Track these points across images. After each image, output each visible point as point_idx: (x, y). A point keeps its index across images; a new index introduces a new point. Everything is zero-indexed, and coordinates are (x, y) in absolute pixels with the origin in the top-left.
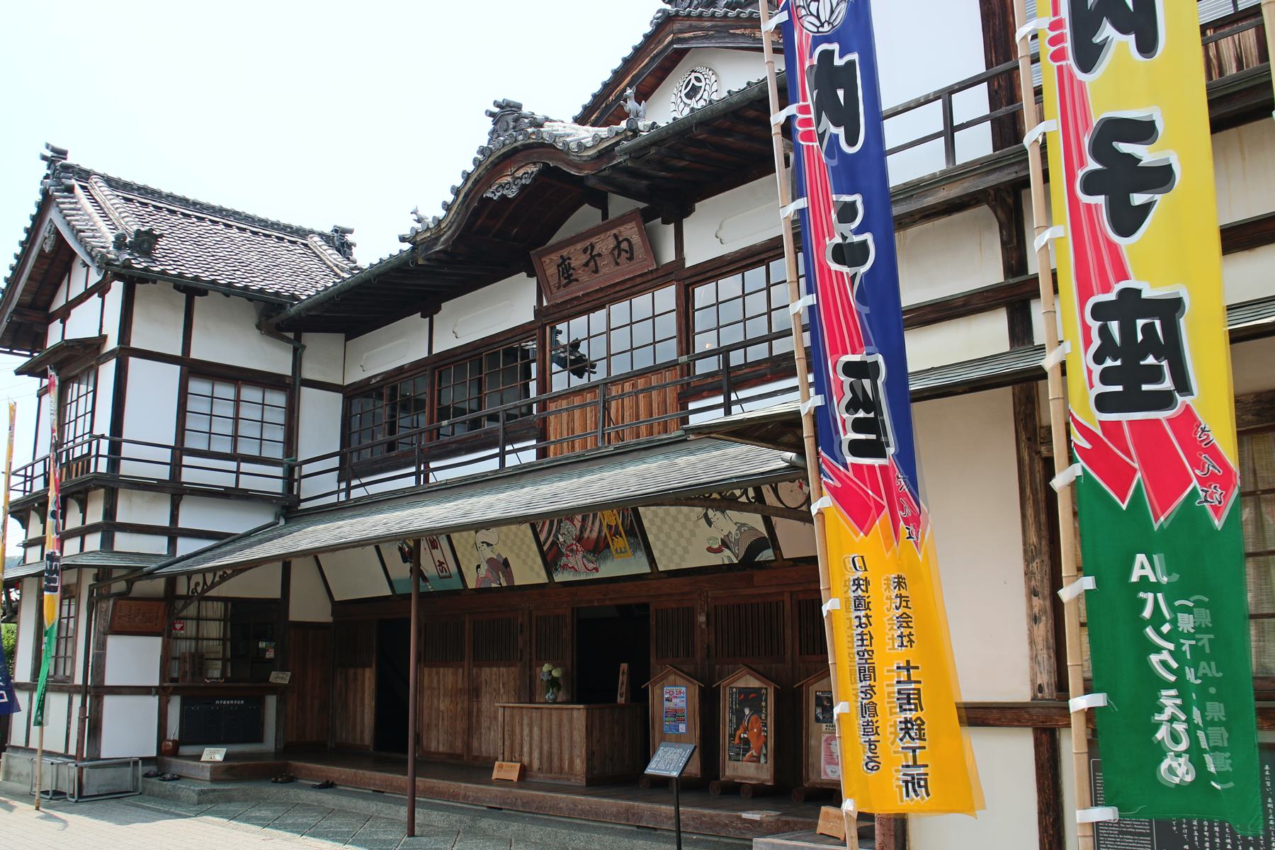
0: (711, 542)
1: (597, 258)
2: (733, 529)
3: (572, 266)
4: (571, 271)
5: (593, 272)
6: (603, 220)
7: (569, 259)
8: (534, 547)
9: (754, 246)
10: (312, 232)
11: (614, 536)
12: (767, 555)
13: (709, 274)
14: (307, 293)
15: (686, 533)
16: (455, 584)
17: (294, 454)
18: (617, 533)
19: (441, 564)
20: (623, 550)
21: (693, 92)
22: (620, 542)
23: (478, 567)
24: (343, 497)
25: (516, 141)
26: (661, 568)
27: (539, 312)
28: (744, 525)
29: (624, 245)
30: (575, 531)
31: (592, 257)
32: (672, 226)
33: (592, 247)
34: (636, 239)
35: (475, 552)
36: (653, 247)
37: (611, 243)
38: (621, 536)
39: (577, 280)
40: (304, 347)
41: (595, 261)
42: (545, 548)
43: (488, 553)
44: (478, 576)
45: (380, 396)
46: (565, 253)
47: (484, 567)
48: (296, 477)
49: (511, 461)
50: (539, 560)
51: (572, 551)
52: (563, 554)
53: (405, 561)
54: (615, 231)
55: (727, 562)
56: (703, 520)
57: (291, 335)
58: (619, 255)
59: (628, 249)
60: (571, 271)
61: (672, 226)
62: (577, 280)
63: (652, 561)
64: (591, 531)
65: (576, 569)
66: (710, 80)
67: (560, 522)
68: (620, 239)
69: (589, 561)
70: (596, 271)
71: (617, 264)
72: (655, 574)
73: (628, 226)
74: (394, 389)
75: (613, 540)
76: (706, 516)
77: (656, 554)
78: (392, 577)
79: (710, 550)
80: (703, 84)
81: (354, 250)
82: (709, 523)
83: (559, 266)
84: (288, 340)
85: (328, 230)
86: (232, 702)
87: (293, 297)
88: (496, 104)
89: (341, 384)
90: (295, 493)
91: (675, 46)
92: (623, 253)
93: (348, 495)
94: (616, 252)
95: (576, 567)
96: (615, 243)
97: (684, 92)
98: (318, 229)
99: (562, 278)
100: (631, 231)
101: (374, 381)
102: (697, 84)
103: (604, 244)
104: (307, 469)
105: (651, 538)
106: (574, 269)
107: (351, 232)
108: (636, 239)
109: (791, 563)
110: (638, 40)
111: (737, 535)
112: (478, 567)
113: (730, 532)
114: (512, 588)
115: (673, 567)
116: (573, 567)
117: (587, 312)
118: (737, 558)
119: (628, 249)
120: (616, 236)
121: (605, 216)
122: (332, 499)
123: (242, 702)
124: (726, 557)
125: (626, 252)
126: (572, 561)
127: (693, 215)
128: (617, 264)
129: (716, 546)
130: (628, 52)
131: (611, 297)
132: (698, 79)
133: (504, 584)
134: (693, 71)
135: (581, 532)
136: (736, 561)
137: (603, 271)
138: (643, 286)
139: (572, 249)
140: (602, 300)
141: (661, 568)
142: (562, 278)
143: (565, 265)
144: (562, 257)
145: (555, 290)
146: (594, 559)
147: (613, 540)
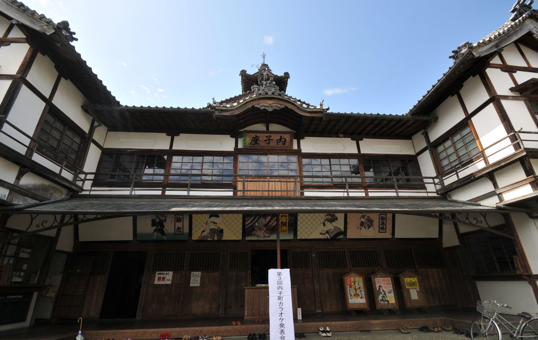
0: (322, 231)
2: (332, 228)
3: (259, 139)
4: (258, 141)
5: (267, 144)
7: (259, 137)
12: (342, 237)
20: (285, 231)
23: (204, 231)
28: (336, 227)
29: (283, 140)
31: (269, 139)
33: (270, 136)
38: (286, 226)
39: (259, 144)
41: (269, 141)
42: (246, 227)
43: (213, 226)
46: (258, 135)
50: (241, 231)
52: (255, 230)
53: (153, 225)
54: (281, 135)
55: (326, 238)
56: (323, 224)
58: (280, 142)
59: (284, 141)
60: (258, 141)
62: (259, 144)
64: (273, 223)
65: (260, 235)
68: (282, 138)
69: (267, 233)
70: (269, 144)
72: (295, 240)
73: (287, 135)
75: (281, 227)
79: (321, 234)
82: (324, 225)
83: (253, 138)
86: (16, 296)
92: (281, 142)
94: (279, 141)
96: (280, 138)
99: (253, 142)
101: (129, 151)
109: (348, 240)
112: (204, 231)
113: (331, 229)
118: (330, 237)
120: (281, 136)
123: (22, 296)
124: (327, 236)
125: (283, 142)
126: (258, 233)
128: (278, 144)
136: (329, 238)
140: (267, 153)
144: (256, 136)
146: (270, 233)
147: (281, 227)
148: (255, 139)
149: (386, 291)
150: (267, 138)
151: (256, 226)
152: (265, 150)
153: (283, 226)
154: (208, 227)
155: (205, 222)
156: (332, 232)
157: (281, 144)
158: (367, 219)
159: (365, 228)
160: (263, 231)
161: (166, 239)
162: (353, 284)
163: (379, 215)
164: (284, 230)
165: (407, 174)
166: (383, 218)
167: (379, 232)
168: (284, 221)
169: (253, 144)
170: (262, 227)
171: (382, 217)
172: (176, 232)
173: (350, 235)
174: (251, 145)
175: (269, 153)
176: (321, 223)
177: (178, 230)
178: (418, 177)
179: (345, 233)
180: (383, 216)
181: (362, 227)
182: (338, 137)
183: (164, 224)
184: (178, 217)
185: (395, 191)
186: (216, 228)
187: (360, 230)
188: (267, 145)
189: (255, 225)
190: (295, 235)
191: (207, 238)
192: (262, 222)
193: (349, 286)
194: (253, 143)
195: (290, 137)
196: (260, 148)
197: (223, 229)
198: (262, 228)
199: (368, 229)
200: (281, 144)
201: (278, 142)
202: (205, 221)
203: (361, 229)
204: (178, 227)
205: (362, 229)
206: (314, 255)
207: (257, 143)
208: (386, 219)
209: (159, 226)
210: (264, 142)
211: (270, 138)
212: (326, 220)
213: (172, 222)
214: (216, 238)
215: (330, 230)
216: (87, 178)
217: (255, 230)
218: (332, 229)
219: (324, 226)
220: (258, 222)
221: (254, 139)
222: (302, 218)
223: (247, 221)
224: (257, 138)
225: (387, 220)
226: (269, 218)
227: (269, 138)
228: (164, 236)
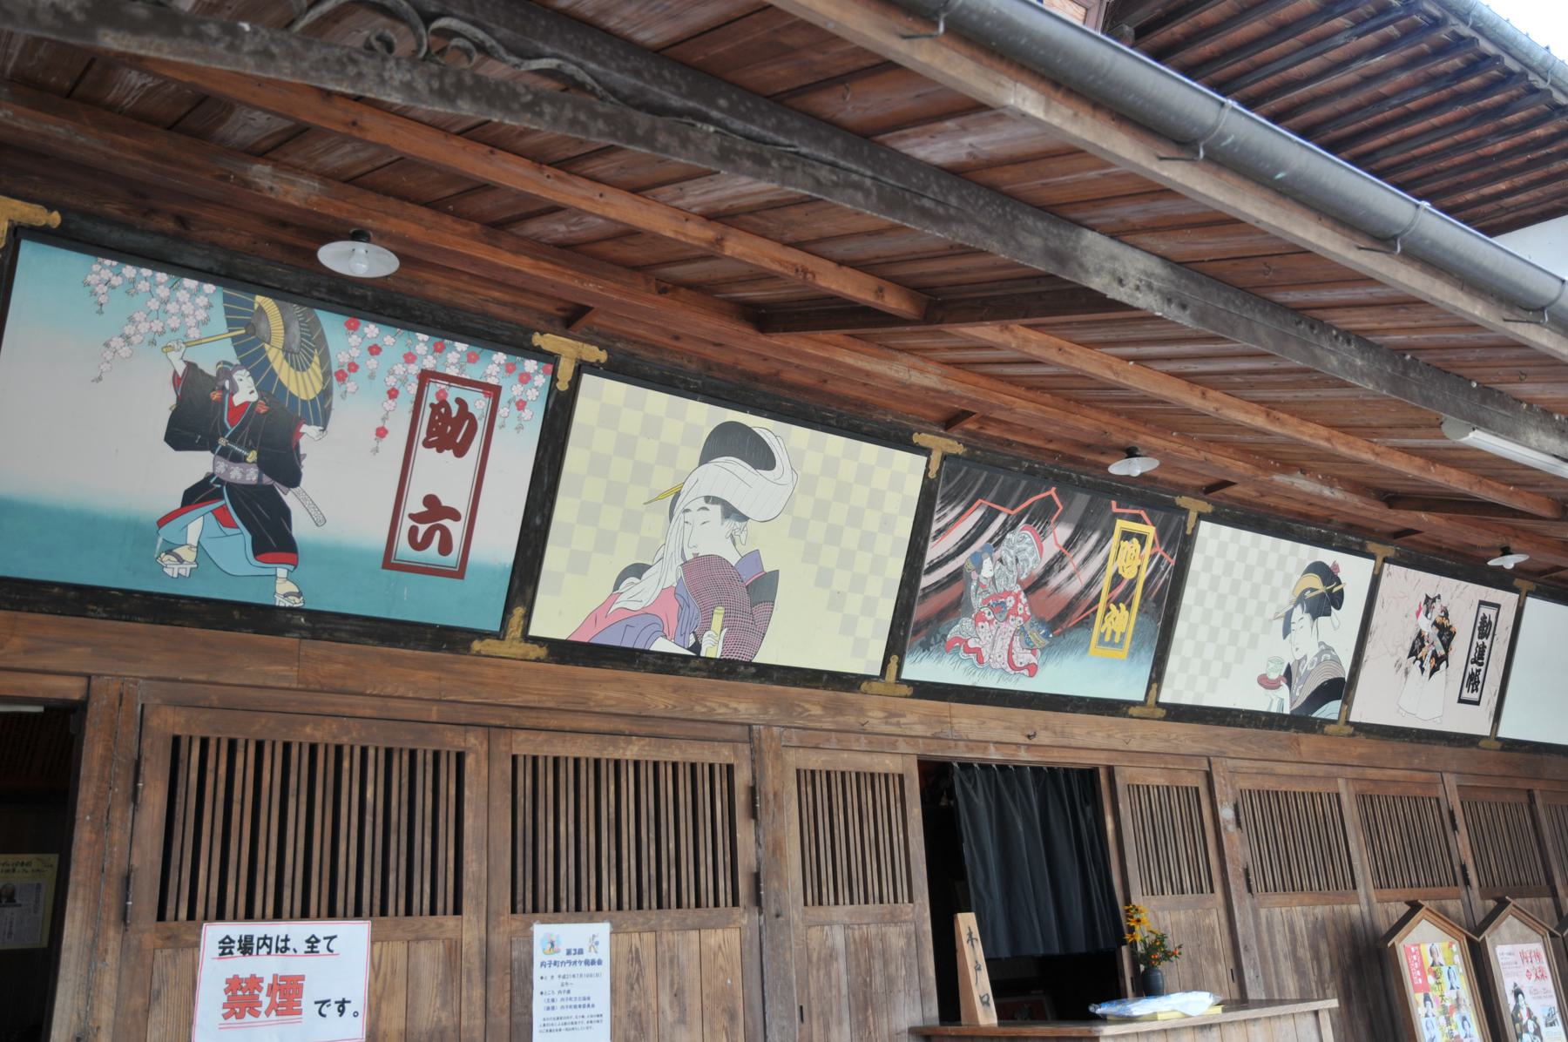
0: (1272, 665)
2: (1312, 651)
11: (1116, 603)
12: (1331, 710)
15: (1244, 638)
18: (1124, 598)
20: (1117, 640)
22: (1121, 621)
23: (638, 570)
28: (1329, 649)
30: (1035, 565)
38: (1129, 607)
42: (926, 581)
47: (664, 576)
64: (1070, 577)
75: (1108, 610)
76: (1288, 617)
82: (1287, 631)
111: (1312, 664)
112: (638, 570)
113: (1305, 657)
116: (977, 651)
124: (1281, 701)
129: (1273, 676)
135: (1049, 570)
147: (1108, 610)
149: (1541, 1014)
151: (979, 584)
153: (1113, 607)
154: (673, 547)
155: (664, 494)
159: (1423, 670)
160: (1015, 623)
161: (296, 602)
162: (1431, 980)
164: (1113, 633)
167: (1461, 701)
168: (1128, 575)
170: (1010, 593)
173: (1368, 707)
177: (423, 528)
184: (443, 403)
186: (733, 559)
189: (974, 575)
190: (1157, 675)
191: (652, 638)
192: (1017, 560)
193: (1419, 997)
197: (775, 574)
202: (663, 481)
204: (431, 501)
206: (1226, 813)
209: (252, 456)
213: (381, 433)
214: (712, 648)
215: (1299, 662)
220: (997, 555)
223: (940, 531)
226: (1063, 532)
228: (282, 572)
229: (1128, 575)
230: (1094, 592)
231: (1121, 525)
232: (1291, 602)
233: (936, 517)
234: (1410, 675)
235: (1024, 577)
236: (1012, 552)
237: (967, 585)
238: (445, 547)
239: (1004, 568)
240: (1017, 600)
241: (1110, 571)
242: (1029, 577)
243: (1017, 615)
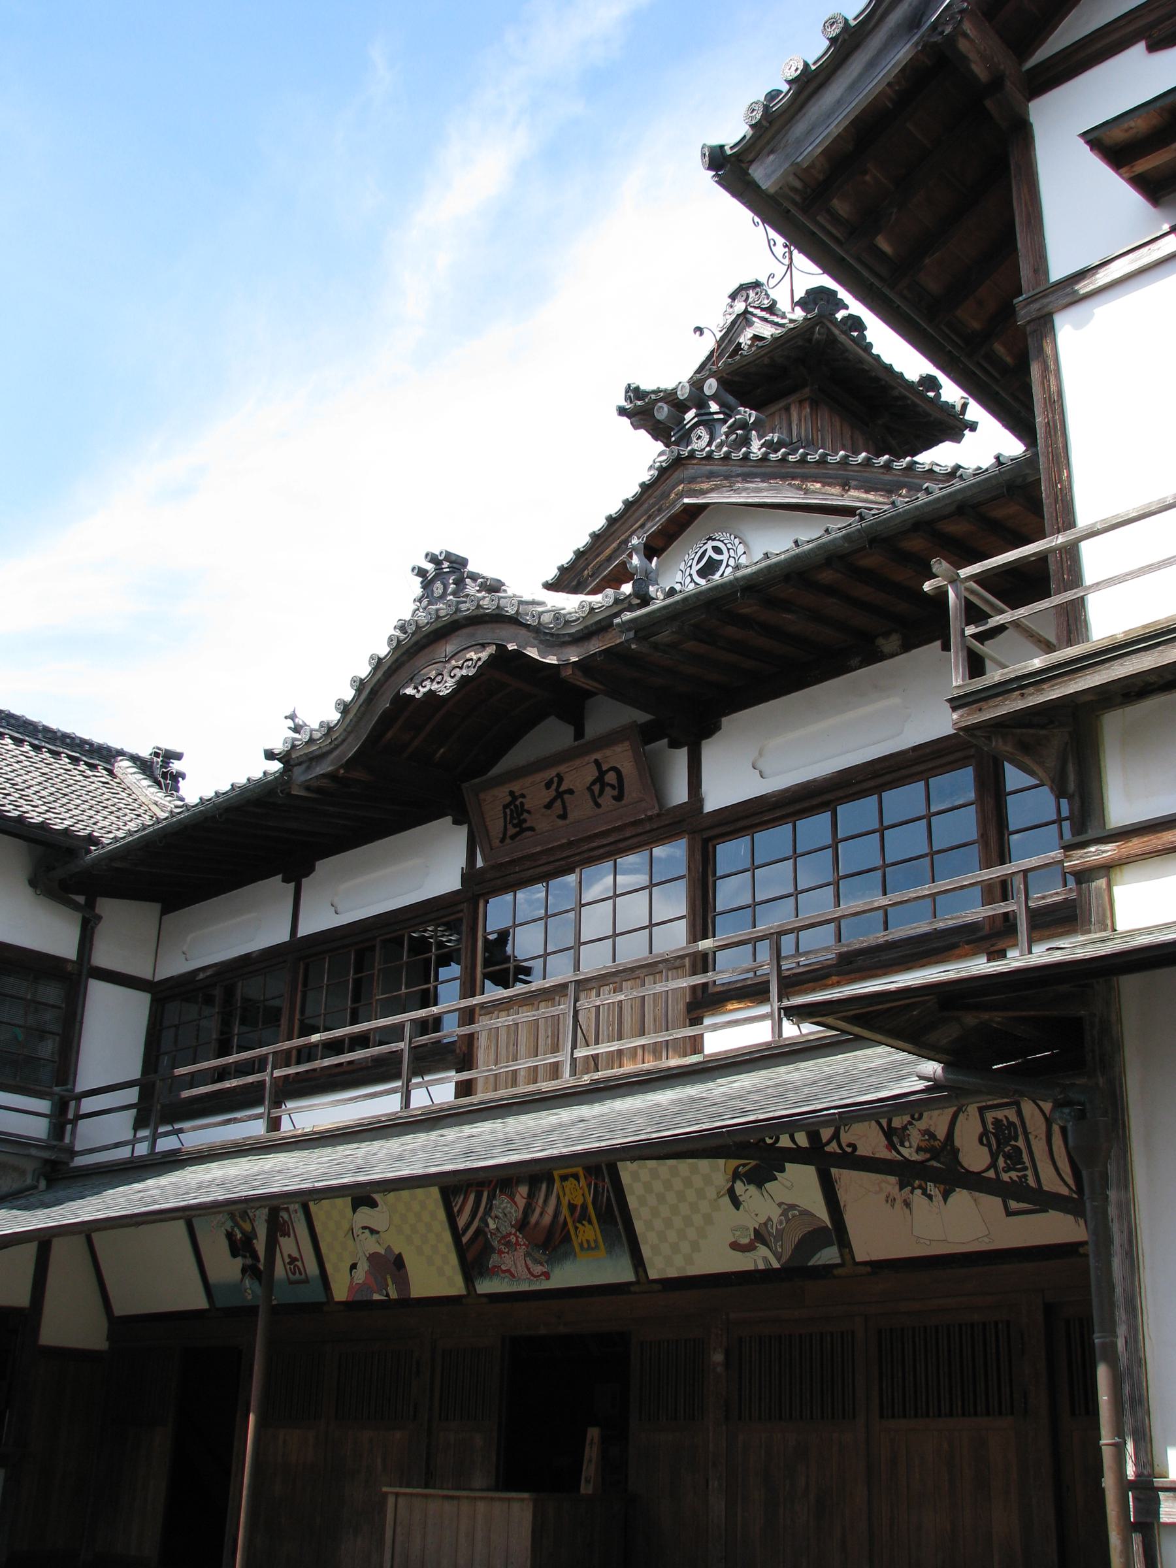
0: (737, 1233)
1: (566, 796)
2: (775, 1213)
4: (525, 815)
5: (559, 817)
6: (576, 739)
7: (523, 796)
8: (447, 1237)
9: (814, 781)
10: (121, 753)
11: (580, 1222)
13: (740, 824)
14: (110, 836)
15: (698, 1219)
16: (313, 1294)
17: (71, 1082)
18: (584, 1217)
19: (293, 1260)
20: (593, 1245)
21: (710, 568)
22: (589, 1232)
23: (354, 1267)
24: (142, 1149)
25: (458, 610)
26: (653, 1274)
27: (469, 875)
28: (792, 1207)
29: (611, 778)
30: (516, 1213)
31: (560, 795)
32: (685, 750)
33: (561, 779)
34: (627, 767)
35: (350, 1242)
36: (654, 780)
37: (591, 774)
38: (590, 1222)
39: (532, 829)
40: (99, 918)
42: (465, 1239)
43: (371, 1245)
44: (352, 1279)
45: (209, 1000)
46: (516, 787)
47: (363, 1267)
48: (70, 1116)
49: (419, 1100)
51: (508, 1244)
52: (493, 1250)
53: (234, 1254)
54: (597, 756)
55: (761, 1266)
56: (727, 1199)
57: (81, 899)
59: (614, 782)
60: (525, 815)
61: (685, 750)
62: (532, 829)
63: (638, 1262)
64: (541, 1214)
66: (736, 552)
67: (491, 1198)
68: (605, 768)
69: (537, 1262)
70: (563, 816)
71: (598, 805)
73: (618, 749)
74: (230, 992)
75: (576, 1228)
76: (731, 1192)
77: (646, 1251)
78: (212, 1278)
79: (735, 1246)
80: (724, 557)
81: (182, 784)
82: (736, 1203)
84: (75, 906)
85: (145, 753)
87: (91, 840)
88: (433, 559)
89: (149, 977)
90: (67, 1140)
91: (686, 501)
92: (608, 789)
93: (153, 1145)
94: (596, 788)
95: (513, 1270)
97: (695, 568)
98: (130, 749)
99: (509, 826)
100: (621, 757)
101: (201, 976)
102: (717, 557)
103: (580, 776)
104: (88, 1105)
105: (639, 1226)
106: (529, 812)
107: (179, 756)
108: (627, 767)
109: (869, 1269)
110: (631, 490)
111: (781, 1222)
112: (354, 1267)
113: (770, 1219)
114: (407, 1303)
115: (672, 1273)
116: (508, 1271)
117: (545, 877)
118: (779, 1259)
119: (614, 782)
120: (597, 763)
121: (579, 734)
122: (124, 1153)
124: (761, 1258)
125: (613, 787)
127: (717, 734)
129: (745, 1241)
130: (615, 507)
131: (586, 855)
132: (717, 550)
133: (394, 1295)
134: (710, 539)
137: (573, 815)
138: (635, 840)
139: (528, 780)
141: (653, 1274)
142: (509, 826)
143: (516, 806)
144: (512, 793)
145: (496, 843)
146: (544, 1258)
147: (576, 1228)
148: (511, 810)
150: (552, 793)
152: (561, 847)
153: (578, 1225)
154: (361, 1254)
155: (349, 1231)
156: (780, 1234)
157: (607, 800)
158: (923, 1144)
159: (930, 1197)
163: (981, 1110)
164: (588, 1241)
165: (319, 1015)
166: (1008, 1128)
167: (1009, 1213)
168: (579, 1202)
169: (513, 837)
170: (510, 1234)
171: (997, 1122)
172: (290, 1274)
174: (508, 841)
175: (577, 858)
176: (719, 1196)
178: (348, 1021)
179: (839, 1232)
180: (1000, 1114)
181: (912, 1192)
182: (873, 656)
183: (255, 1245)
185: (69, 1127)
187: (908, 1211)
188: (561, 822)
189: (487, 1229)
192: (505, 1215)
194: (512, 831)
195: (630, 753)
196: (538, 849)
198: (513, 1238)
199: (945, 1198)
200: (607, 800)
201: (597, 793)
202: (346, 1226)
203: (907, 1204)
205: (914, 1206)
206: (718, 1357)
207: (524, 826)
208: (1026, 1134)
209: (248, 1255)
210: (549, 812)
211: (561, 789)
212: (736, 1176)
215: (765, 1224)
216: (81, 1112)
217: (493, 1250)
218: (775, 1221)
219: (738, 1209)
220: (493, 1214)
221: (508, 811)
222: (635, 1176)
224: (518, 803)
225: (1031, 1137)
226: (523, 1190)
227: (557, 790)
229: (579, 1202)
230: (561, 1219)
231: (556, 1174)
232: (727, 1181)
233: (453, 1204)
234: (896, 1205)
235: (513, 1222)
236: (500, 1210)
237: (486, 1234)
238: (300, 1273)
239: (500, 1221)
240: (517, 1237)
241: (565, 1203)
242: (517, 1221)
243: (521, 1245)
